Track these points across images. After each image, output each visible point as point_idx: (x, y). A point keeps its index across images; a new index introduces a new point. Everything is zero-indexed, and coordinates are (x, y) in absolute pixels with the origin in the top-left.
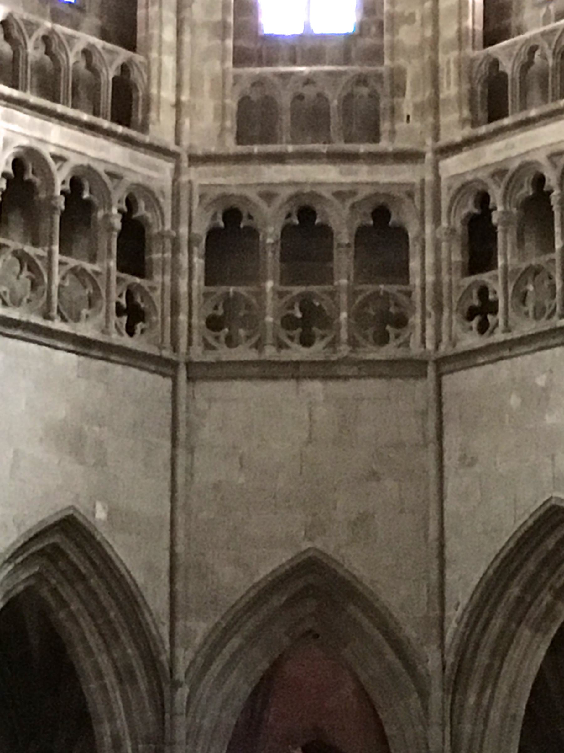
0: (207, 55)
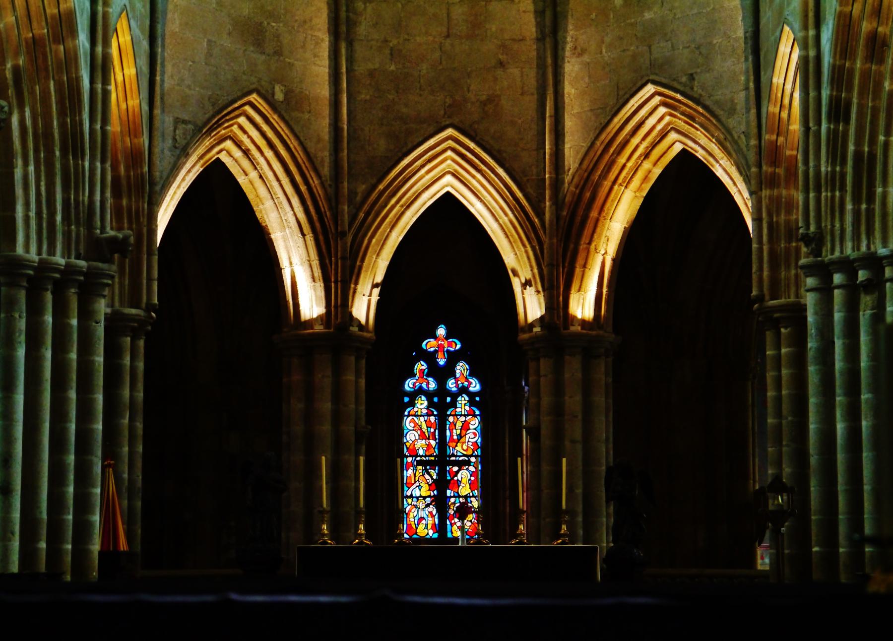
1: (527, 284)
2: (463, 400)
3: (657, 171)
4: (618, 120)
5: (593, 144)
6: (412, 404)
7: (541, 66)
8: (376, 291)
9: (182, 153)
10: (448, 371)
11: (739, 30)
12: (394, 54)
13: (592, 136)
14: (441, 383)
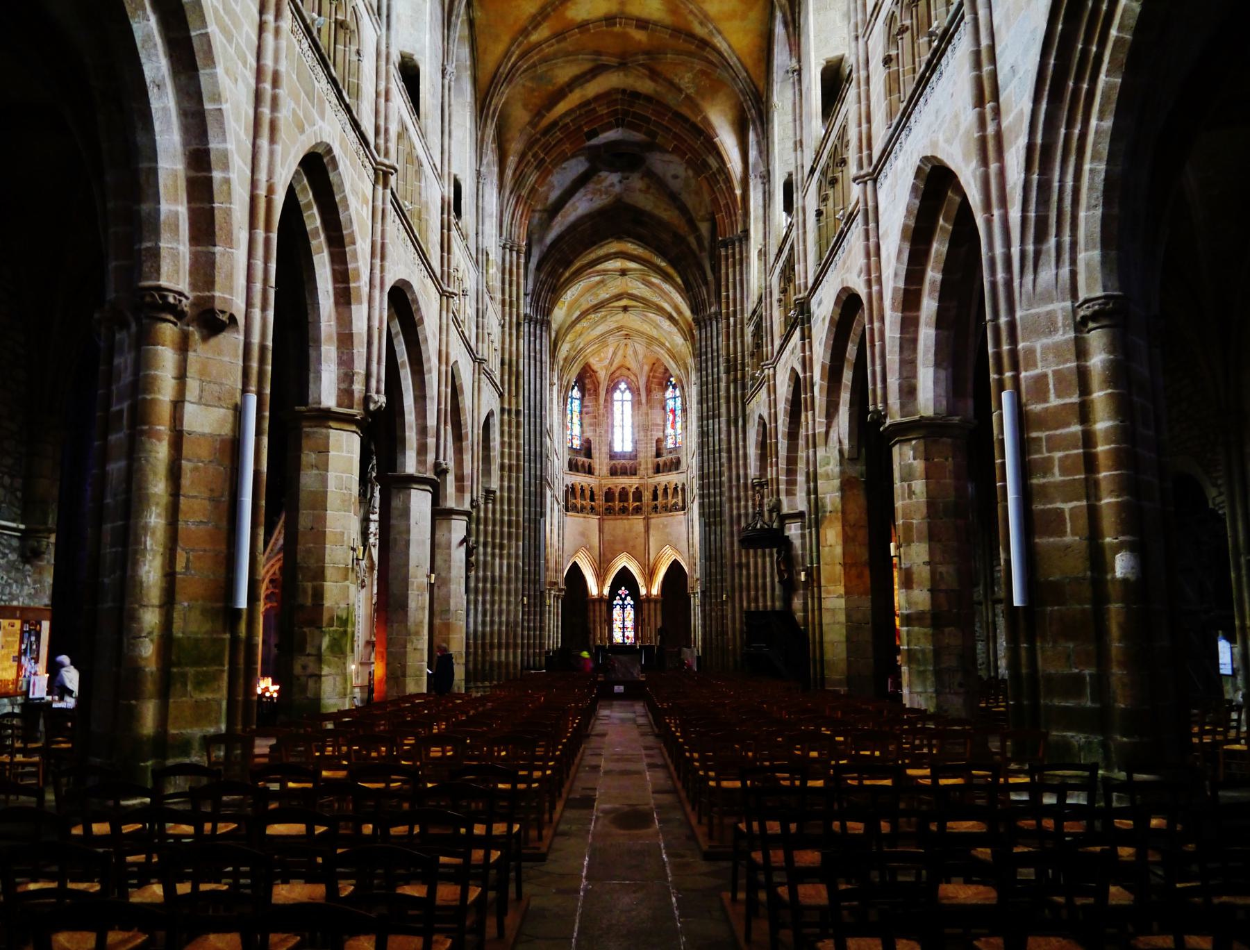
2: (629, 607)
10: (625, 599)
11: (686, 536)
12: (613, 536)
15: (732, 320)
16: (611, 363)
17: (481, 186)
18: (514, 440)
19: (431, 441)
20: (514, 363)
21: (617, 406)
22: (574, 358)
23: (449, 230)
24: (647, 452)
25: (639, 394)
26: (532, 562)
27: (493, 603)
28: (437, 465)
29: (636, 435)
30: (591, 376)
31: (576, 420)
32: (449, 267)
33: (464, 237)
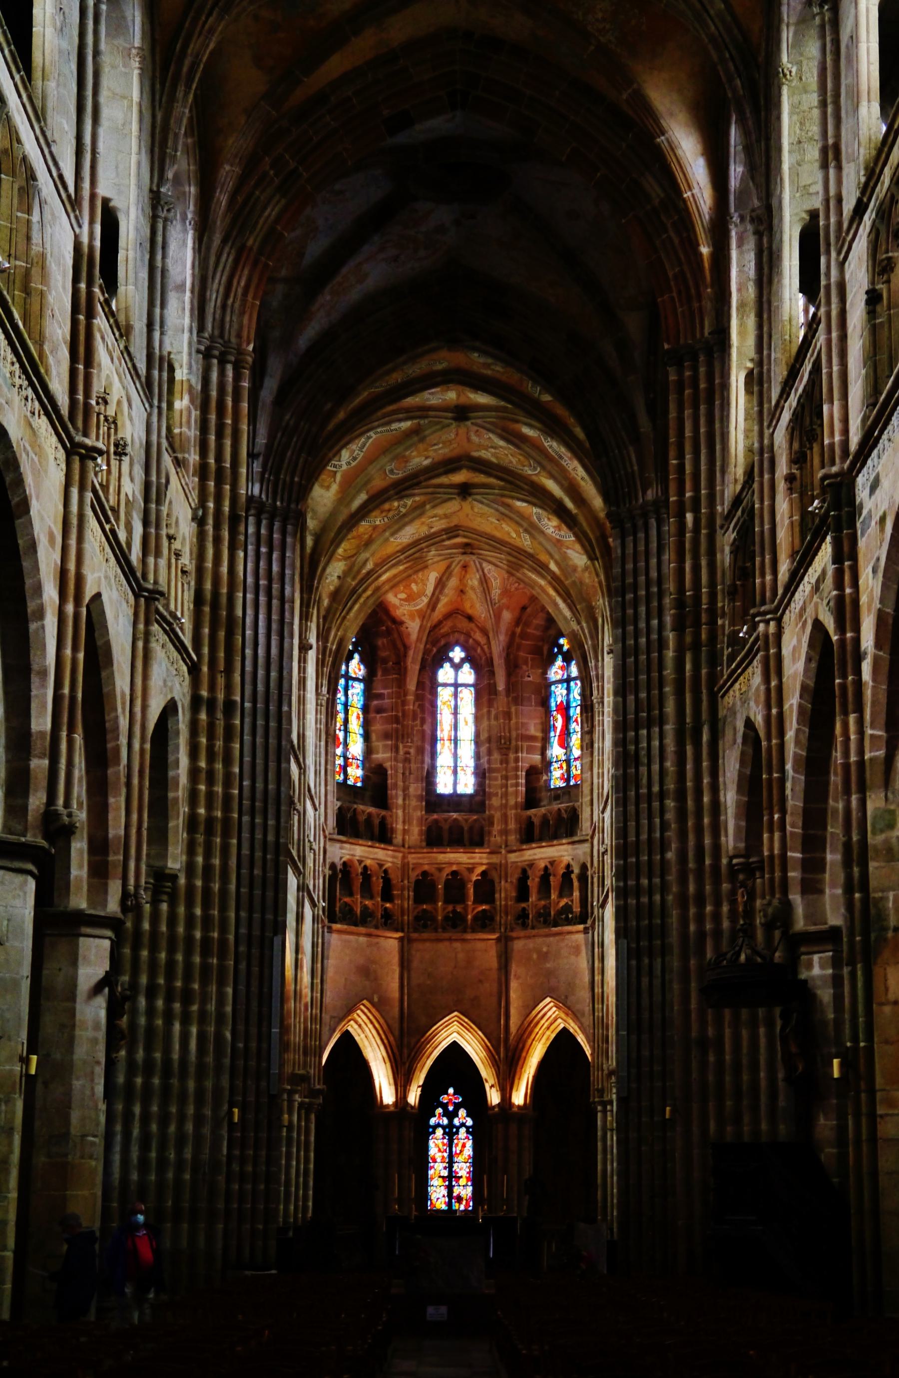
0: (415, 809)
1: (492, 1086)
2: (463, 1130)
3: (553, 1036)
4: (534, 1013)
5: (523, 1023)
6: (434, 1132)
7: (499, 980)
8: (420, 1089)
9: (333, 1031)
10: (455, 1114)
11: (586, 978)
13: (523, 1018)
14: (451, 1120)
15: (689, 517)
16: (433, 604)
17: (160, 226)
18: (219, 766)
19: (39, 764)
20: (224, 600)
21: (444, 695)
22: (354, 591)
23: (90, 315)
24: (506, 795)
25: (492, 673)
26: (254, 1031)
27: (164, 1120)
28: (49, 816)
29: (484, 760)
30: (389, 632)
31: (355, 725)
32: (87, 395)
33: (123, 331)
